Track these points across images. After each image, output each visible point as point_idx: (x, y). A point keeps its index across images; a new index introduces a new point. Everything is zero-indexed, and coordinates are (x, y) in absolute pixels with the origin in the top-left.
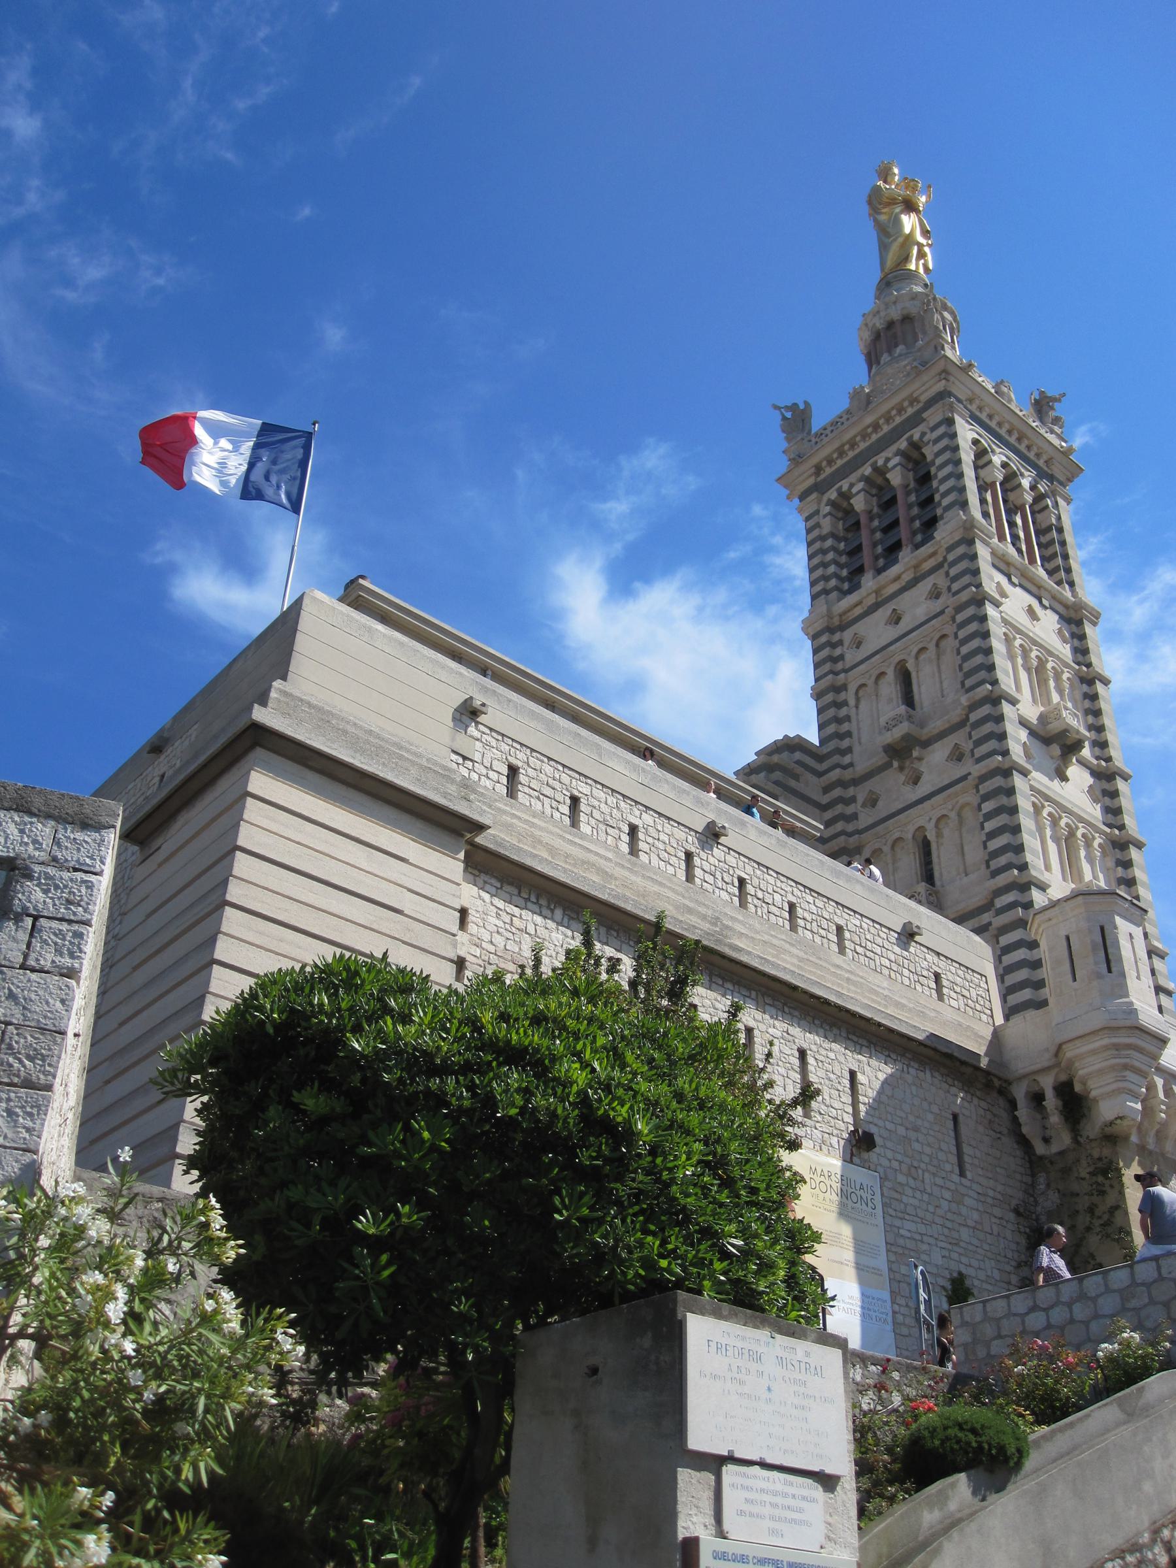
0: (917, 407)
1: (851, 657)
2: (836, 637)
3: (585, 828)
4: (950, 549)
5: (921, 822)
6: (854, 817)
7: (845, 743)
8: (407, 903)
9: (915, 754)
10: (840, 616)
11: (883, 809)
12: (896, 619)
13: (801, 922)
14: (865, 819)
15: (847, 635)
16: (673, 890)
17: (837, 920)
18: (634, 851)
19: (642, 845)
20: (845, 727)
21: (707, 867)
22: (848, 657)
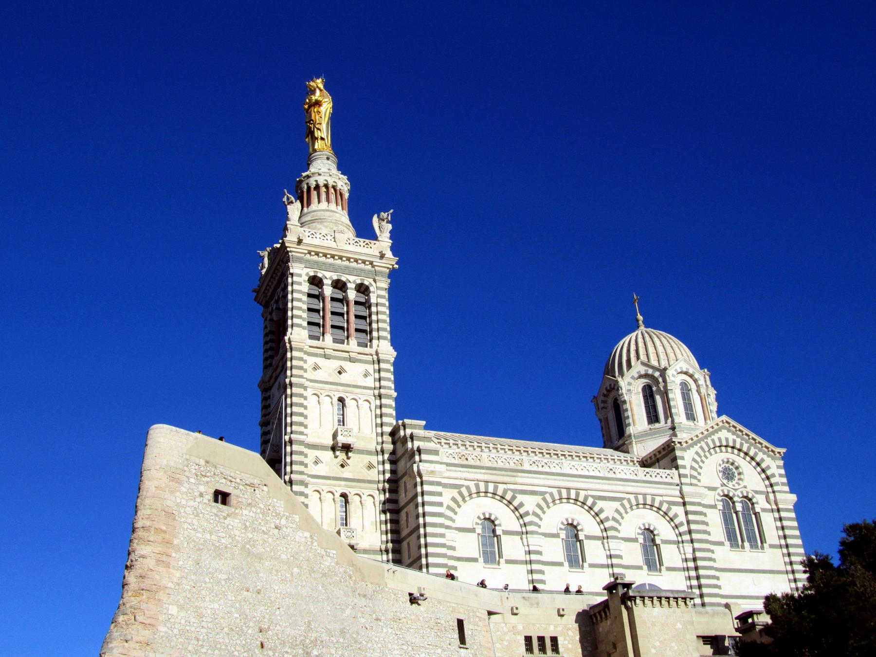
22: (271, 405)
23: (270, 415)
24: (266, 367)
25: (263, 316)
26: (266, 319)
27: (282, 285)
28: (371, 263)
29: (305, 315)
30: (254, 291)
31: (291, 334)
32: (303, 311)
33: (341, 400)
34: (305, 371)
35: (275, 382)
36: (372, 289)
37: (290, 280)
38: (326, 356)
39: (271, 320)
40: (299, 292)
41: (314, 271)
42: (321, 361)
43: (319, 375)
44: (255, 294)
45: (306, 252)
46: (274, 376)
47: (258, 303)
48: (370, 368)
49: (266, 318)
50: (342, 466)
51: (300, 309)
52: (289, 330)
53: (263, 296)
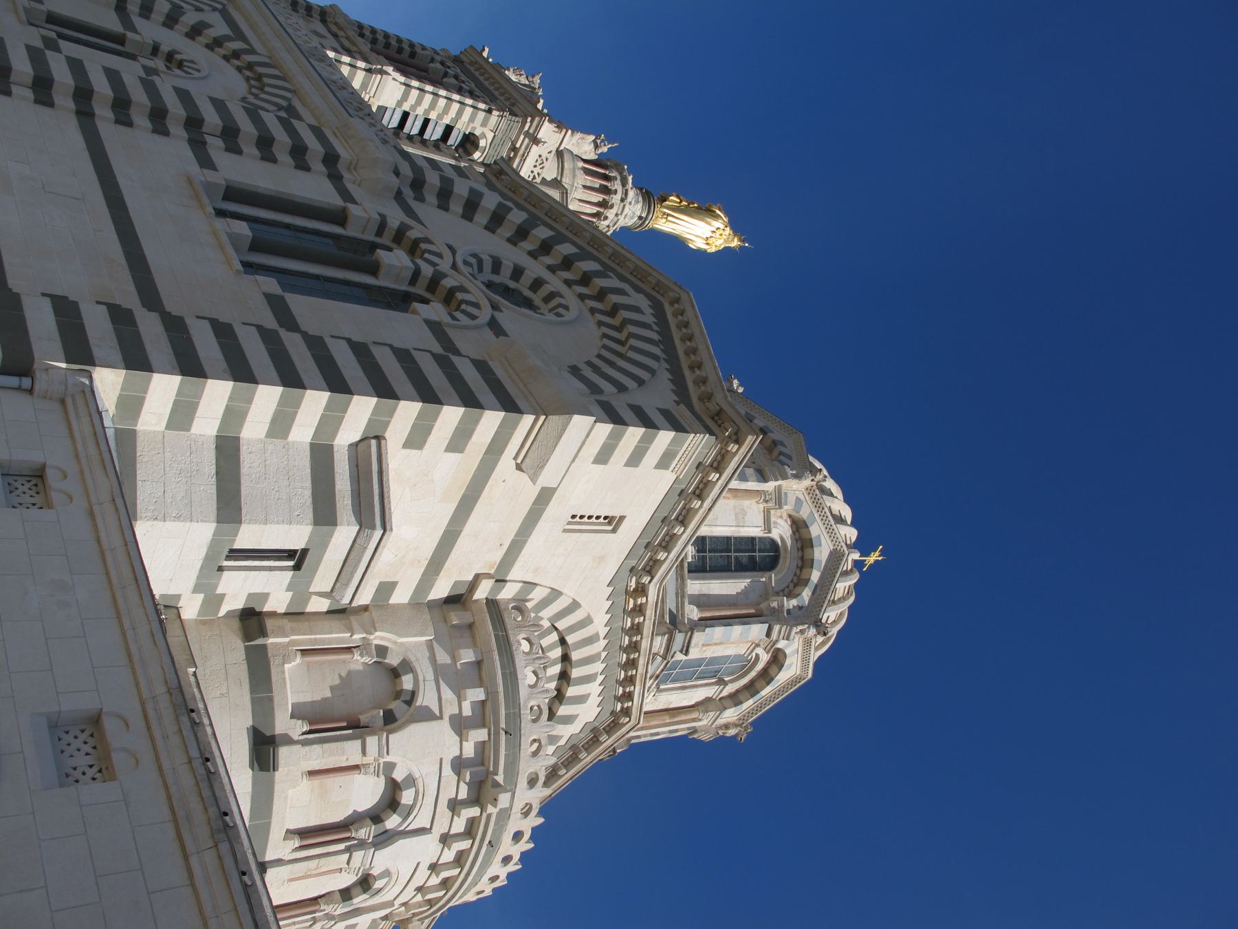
24: (360, 27)
25: (443, 50)
26: (436, 52)
27: (478, 92)
29: (420, 111)
31: (394, 79)
32: (427, 112)
35: (330, 31)
37: (482, 106)
39: (432, 60)
40: (460, 114)
41: (486, 147)
45: (518, 146)
46: (341, 33)
47: (465, 50)
49: (438, 54)
51: (433, 106)
52: (402, 79)
53: (473, 60)
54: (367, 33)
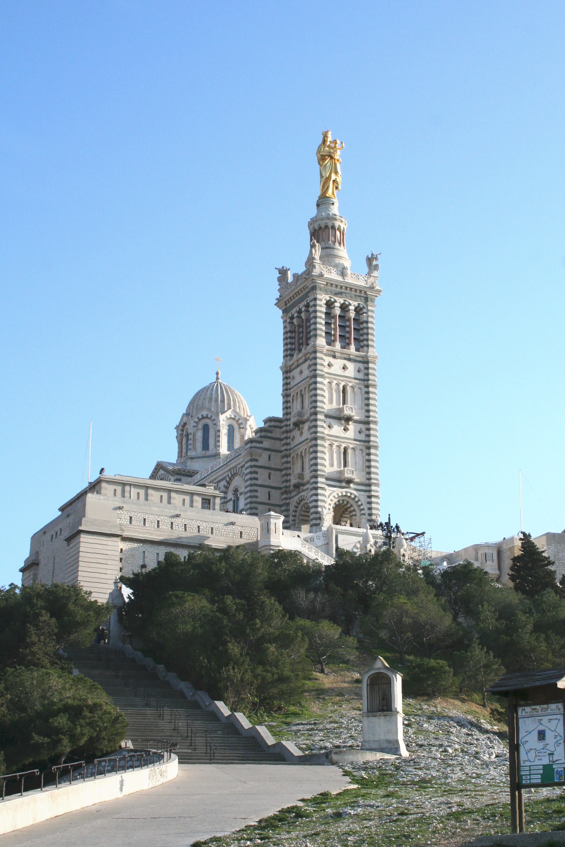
0: (307, 290)
1: (293, 384)
2: (288, 375)
3: (147, 525)
4: (311, 353)
5: (302, 449)
6: (290, 444)
7: (288, 417)
8: (109, 553)
9: (300, 427)
10: (290, 367)
11: (296, 442)
12: (301, 372)
13: (201, 530)
14: (292, 445)
15: (291, 374)
16: (168, 532)
17: (211, 526)
18: (158, 526)
19: (160, 525)
20: (289, 411)
21: (176, 524)
22: (291, 384)
23: (291, 390)
28: (365, 292)
30: (277, 299)
33: (344, 388)
34: (324, 366)
36: (365, 310)
38: (334, 357)
40: (321, 312)
42: (331, 359)
43: (332, 370)
44: (277, 301)
45: (325, 283)
46: (296, 364)
48: (362, 366)
50: (344, 430)
51: (321, 324)
54: (289, 352)
